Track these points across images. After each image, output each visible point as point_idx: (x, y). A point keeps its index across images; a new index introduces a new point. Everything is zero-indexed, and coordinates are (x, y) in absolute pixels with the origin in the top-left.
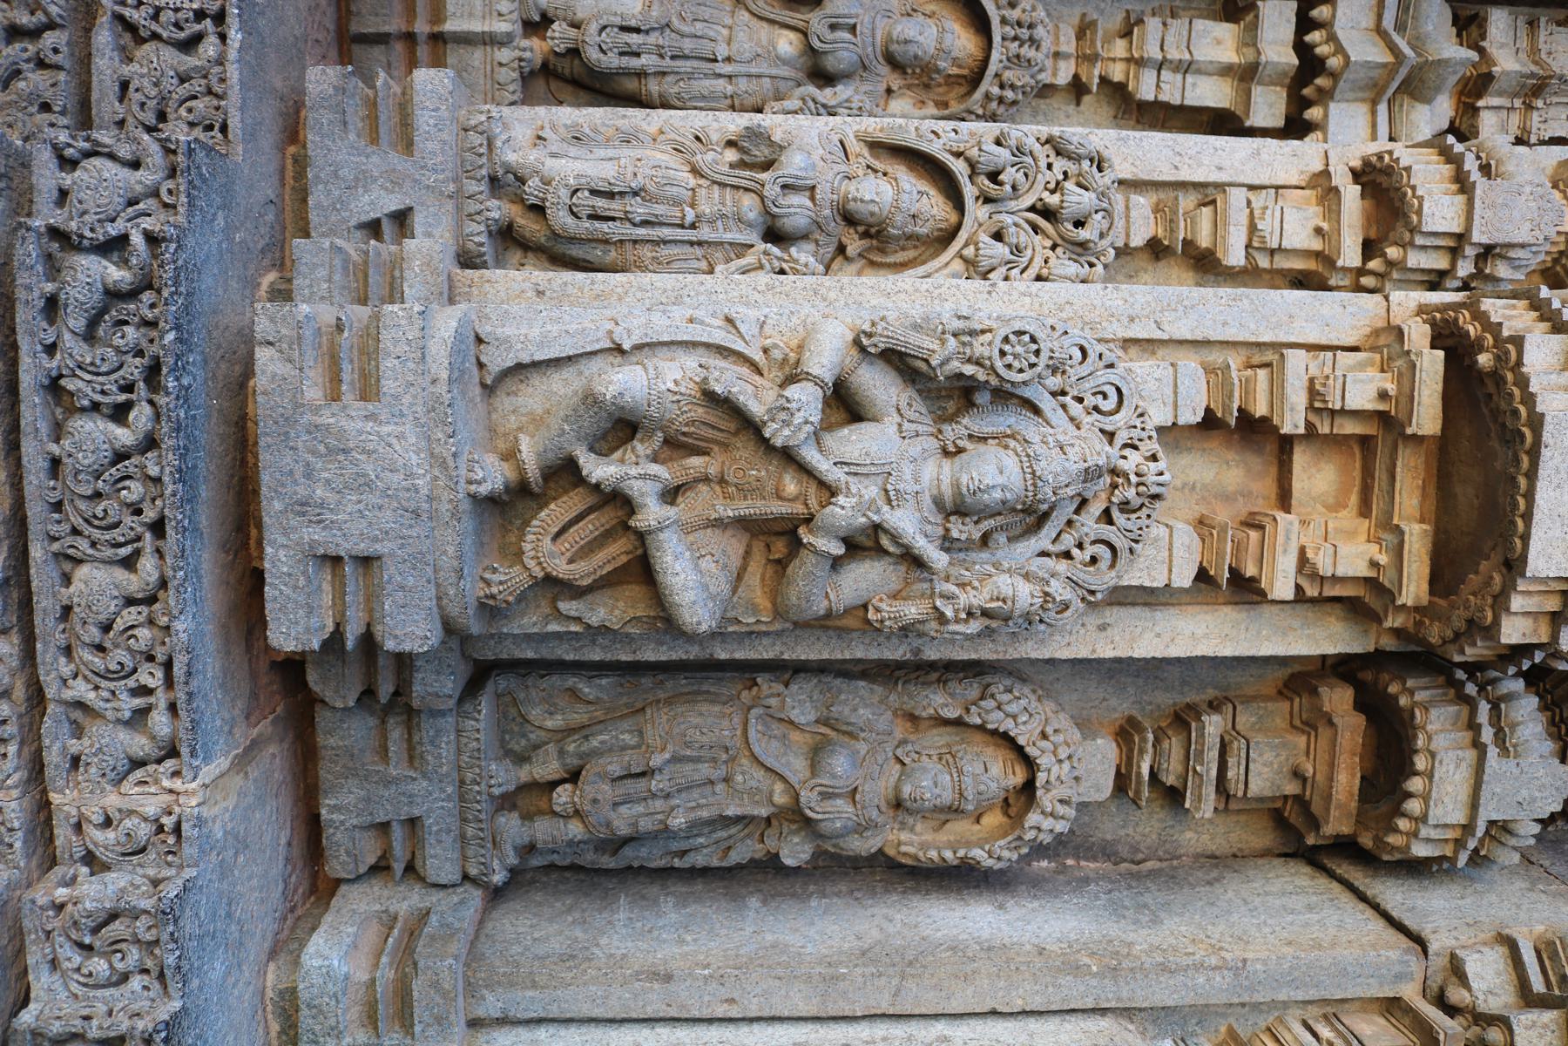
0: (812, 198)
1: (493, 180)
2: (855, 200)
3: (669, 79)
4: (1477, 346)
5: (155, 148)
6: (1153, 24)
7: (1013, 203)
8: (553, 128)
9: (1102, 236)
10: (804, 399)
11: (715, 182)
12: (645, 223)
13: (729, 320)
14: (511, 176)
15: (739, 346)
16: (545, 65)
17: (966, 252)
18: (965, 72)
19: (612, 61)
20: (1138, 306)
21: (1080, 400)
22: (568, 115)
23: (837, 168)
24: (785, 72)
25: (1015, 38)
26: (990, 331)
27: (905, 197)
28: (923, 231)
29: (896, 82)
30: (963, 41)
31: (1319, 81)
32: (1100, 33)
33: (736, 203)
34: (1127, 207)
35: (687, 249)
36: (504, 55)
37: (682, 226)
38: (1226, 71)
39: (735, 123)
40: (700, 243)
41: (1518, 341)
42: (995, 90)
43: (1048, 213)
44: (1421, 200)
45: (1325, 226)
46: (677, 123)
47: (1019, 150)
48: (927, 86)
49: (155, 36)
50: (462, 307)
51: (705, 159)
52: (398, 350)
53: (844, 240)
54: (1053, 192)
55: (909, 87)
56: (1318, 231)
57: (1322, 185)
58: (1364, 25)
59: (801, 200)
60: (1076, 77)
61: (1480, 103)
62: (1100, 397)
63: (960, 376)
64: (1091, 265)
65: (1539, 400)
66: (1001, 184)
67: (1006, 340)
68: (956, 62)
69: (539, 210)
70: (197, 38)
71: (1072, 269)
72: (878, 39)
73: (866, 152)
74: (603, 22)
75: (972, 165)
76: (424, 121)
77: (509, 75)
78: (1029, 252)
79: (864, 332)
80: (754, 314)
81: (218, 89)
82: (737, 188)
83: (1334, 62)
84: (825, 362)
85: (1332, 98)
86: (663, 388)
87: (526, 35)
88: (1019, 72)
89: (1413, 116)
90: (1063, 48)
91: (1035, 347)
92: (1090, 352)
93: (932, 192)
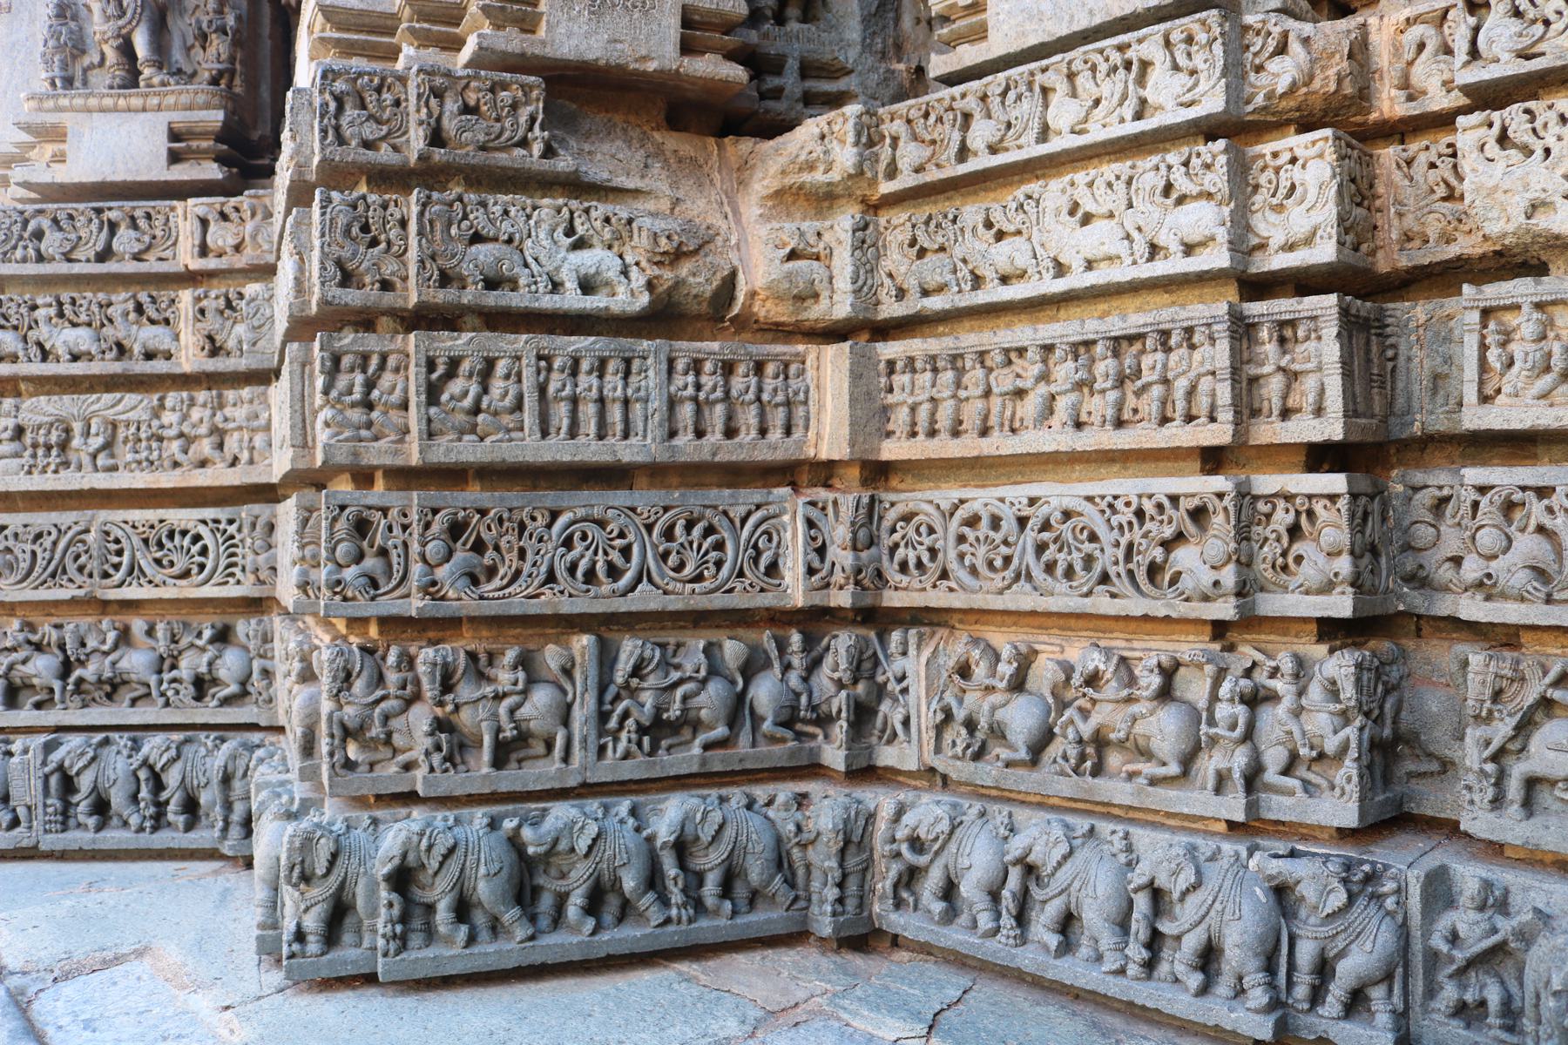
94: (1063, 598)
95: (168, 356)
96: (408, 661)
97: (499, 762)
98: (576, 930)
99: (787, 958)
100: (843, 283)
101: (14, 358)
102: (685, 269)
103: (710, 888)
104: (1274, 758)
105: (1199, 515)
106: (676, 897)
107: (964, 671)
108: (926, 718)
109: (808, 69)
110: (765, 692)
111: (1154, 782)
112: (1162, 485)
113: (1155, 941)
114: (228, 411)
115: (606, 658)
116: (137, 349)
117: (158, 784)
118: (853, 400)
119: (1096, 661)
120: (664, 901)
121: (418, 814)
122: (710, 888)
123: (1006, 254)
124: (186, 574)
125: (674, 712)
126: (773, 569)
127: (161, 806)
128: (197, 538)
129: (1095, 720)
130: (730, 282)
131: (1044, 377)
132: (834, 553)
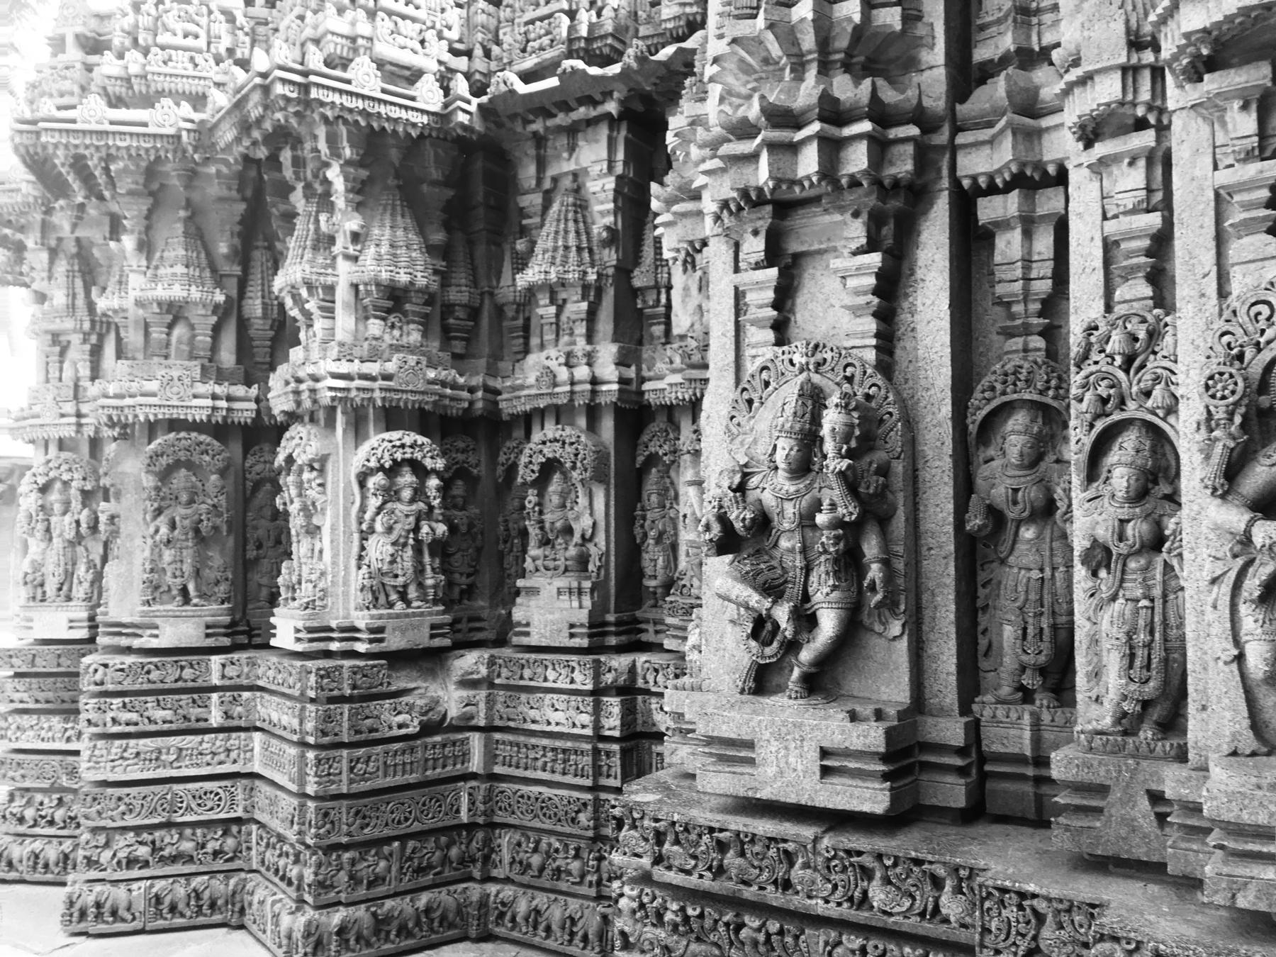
0: (1128, 521)
1: (1125, 733)
2: (1127, 492)
3: (1057, 609)
4: (1198, 56)
5: (1099, 946)
6: (1000, 289)
7: (1124, 385)
8: (1090, 690)
9: (1144, 321)
10: (1262, 535)
11: (1120, 586)
12: (1152, 633)
13: (1214, 581)
14: (1124, 721)
15: (1232, 575)
16: (1054, 691)
17: (1161, 415)
18: (1040, 414)
19: (1046, 646)
20: (1192, 293)
21: (1263, 332)
22: (1081, 680)
23: (1107, 505)
24: (1047, 533)
25: (1015, 384)
26: (1207, 407)
27: (1123, 459)
28: (1148, 443)
29: (1051, 457)
30: (1018, 420)
31: (1028, 173)
32: (1009, 323)
33: (1134, 572)
34: (1125, 302)
35: (1169, 604)
36: (1046, 717)
37: (1153, 608)
38: (1028, 235)
39: (1080, 572)
40: (1165, 596)
41: (1187, 36)
42: (1051, 393)
43: (1128, 361)
44: (1099, 105)
45: (1127, 161)
46: (1083, 608)
47: (1085, 386)
48: (1053, 437)
49: (1035, 938)
50: (1211, 765)
51: (1105, 592)
52: (1236, 810)
53: (1160, 495)
54: (1114, 359)
55: (1054, 447)
56: (1131, 164)
57: (1100, 167)
58: (988, 151)
59: (1130, 529)
60: (1040, 334)
61: (1037, 48)
62: (1260, 318)
63: (1242, 426)
64: (1166, 325)
65: (1228, 13)
66: (1109, 396)
67: (1213, 396)
68: (1033, 421)
69: (1146, 704)
70: (1034, 911)
71: (1168, 339)
72: (1021, 473)
73: (1095, 485)
74: (1020, 651)
75: (1097, 417)
76: (1085, 776)
77: (1060, 716)
78: (1159, 371)
79: (1212, 494)
80: (1208, 565)
81: (1065, 905)
82: (1123, 572)
83: (1014, 169)
84: (1236, 519)
85: (1040, 161)
86: (1259, 631)
87: (1032, 702)
88: (1038, 377)
89: (1048, 99)
90: (1020, 346)
91: (1217, 376)
92: (1224, 329)
93: (1120, 440)
94: (548, 825)
95: (206, 720)
96: (339, 857)
97: (368, 888)
98: (393, 942)
99: (461, 946)
100: (482, 715)
101: (136, 724)
102: (431, 714)
103: (436, 924)
104: (605, 876)
105: (585, 805)
106: (425, 928)
107: (519, 844)
108: (507, 858)
109: (471, 620)
110: (454, 852)
111: (573, 883)
112: (576, 794)
113: (572, 934)
114: (232, 742)
115: (403, 848)
116: (193, 718)
117: (198, 897)
118: (485, 754)
119: (557, 845)
120: (421, 930)
121: (341, 908)
122: (436, 924)
123: (533, 714)
124: (212, 809)
125: (425, 864)
126: (458, 811)
127: (200, 907)
128: (217, 794)
129: (557, 863)
130: (445, 715)
131: (544, 756)
132: (478, 803)
